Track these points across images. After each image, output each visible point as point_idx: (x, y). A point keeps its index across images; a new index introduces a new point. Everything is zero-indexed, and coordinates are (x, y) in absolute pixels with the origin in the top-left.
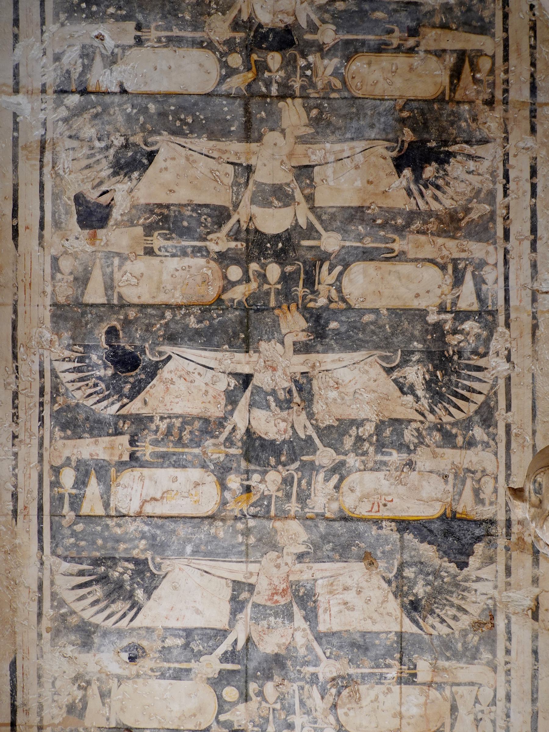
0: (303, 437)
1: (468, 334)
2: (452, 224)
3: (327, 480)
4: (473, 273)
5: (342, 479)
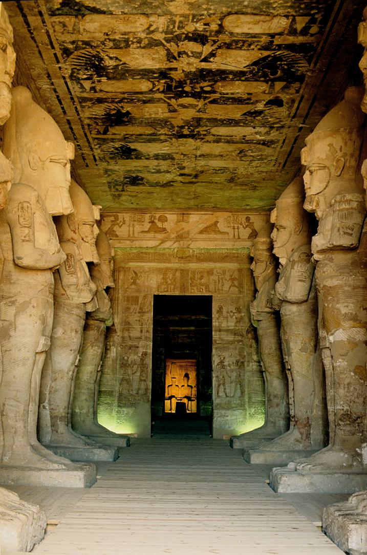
0: (172, 43)
1: (84, 74)
2: (100, 101)
3: (158, 28)
4: (86, 90)
5: (148, 28)
